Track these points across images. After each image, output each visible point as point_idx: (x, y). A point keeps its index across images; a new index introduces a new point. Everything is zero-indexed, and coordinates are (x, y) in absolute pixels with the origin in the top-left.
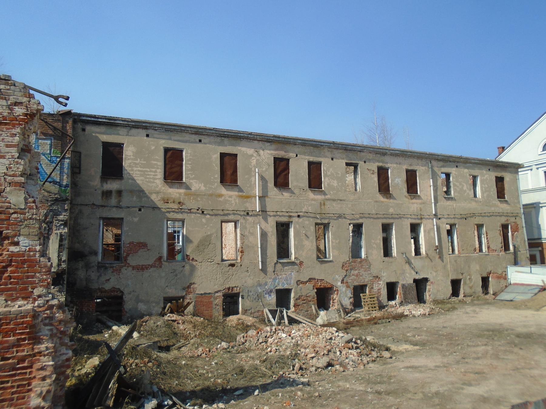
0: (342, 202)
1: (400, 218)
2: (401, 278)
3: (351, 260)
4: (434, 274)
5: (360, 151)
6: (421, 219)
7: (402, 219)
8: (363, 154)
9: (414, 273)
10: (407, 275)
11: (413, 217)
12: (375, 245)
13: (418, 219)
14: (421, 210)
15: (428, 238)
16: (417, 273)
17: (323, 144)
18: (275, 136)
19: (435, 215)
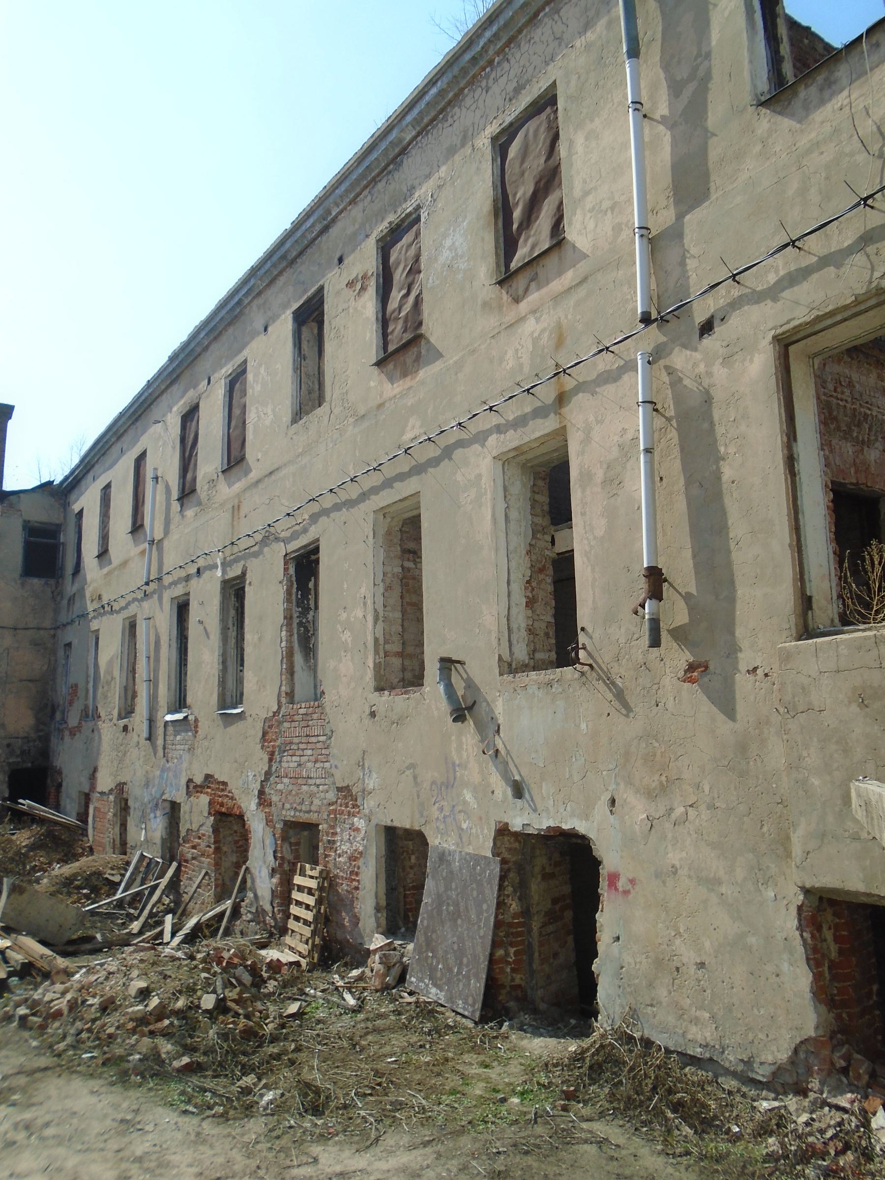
0: (273, 477)
1: (448, 452)
2: (435, 812)
3: (283, 710)
4: (638, 810)
5: (325, 229)
6: (561, 399)
7: (458, 453)
8: (334, 231)
9: (502, 790)
10: (468, 796)
11: (512, 413)
12: (347, 636)
13: (540, 413)
14: (560, 342)
15: (600, 532)
16: (518, 791)
17: (236, 299)
18: (172, 359)
19: (646, 319)
